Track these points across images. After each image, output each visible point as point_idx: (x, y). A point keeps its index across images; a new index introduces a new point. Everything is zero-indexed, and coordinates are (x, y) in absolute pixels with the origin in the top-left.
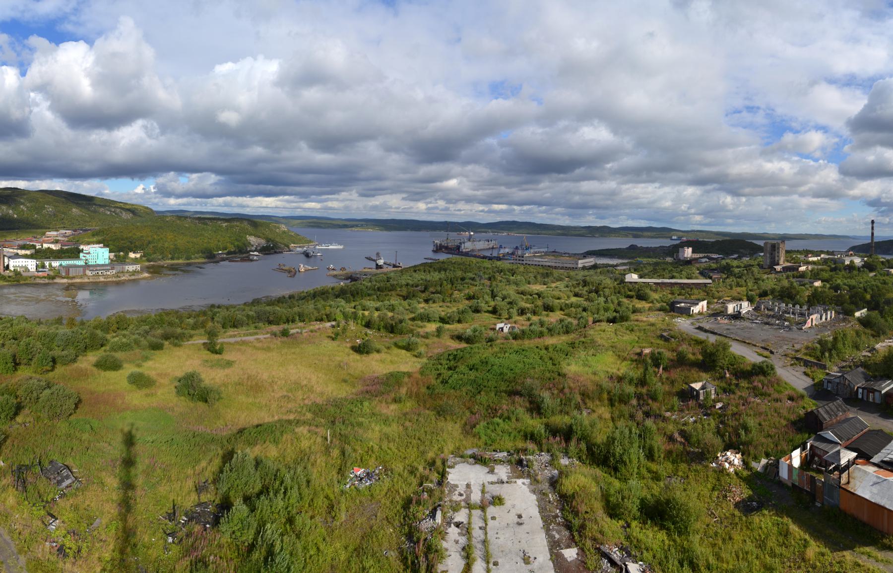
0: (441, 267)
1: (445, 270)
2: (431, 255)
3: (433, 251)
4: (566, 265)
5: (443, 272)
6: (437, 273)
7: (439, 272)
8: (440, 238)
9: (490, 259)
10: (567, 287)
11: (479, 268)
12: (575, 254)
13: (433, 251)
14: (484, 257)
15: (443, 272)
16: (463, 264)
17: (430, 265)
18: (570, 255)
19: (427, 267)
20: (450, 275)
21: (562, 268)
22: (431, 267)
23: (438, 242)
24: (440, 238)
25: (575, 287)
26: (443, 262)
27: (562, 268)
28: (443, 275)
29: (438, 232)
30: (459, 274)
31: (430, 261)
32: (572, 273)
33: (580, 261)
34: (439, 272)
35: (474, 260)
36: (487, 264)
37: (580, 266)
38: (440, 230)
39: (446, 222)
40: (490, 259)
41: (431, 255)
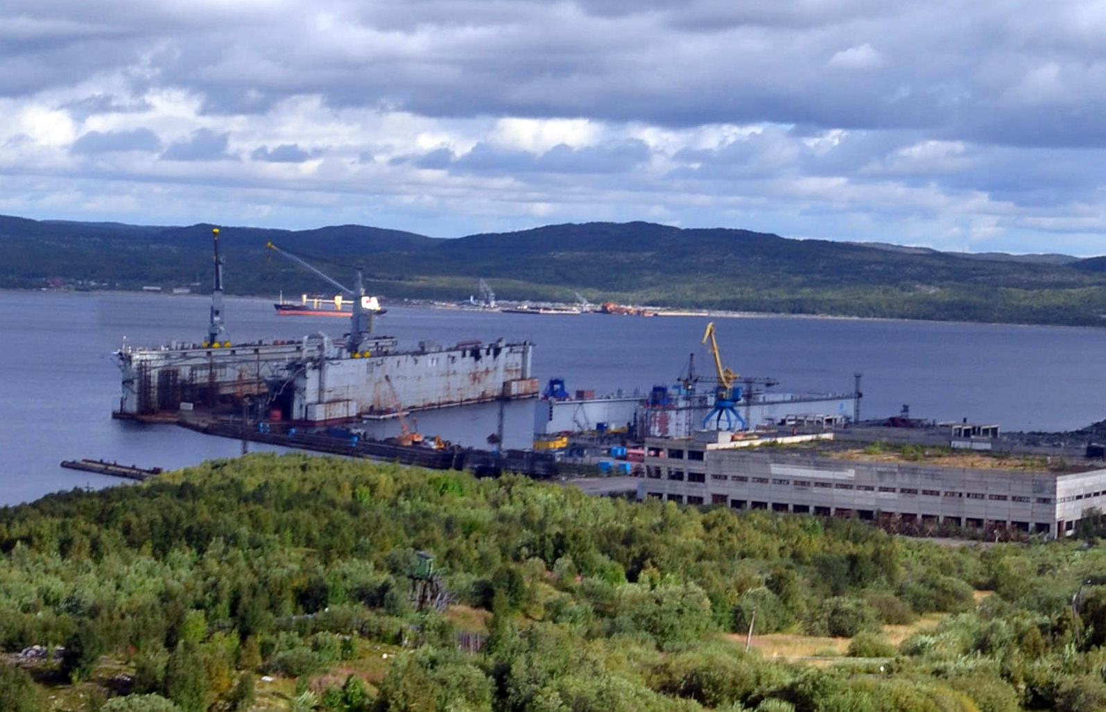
0: (170, 521)
1: (198, 539)
2: (104, 440)
3: (121, 416)
4: (972, 509)
5: (183, 555)
6: (145, 560)
7: (161, 551)
8: (164, 333)
9: (488, 466)
10: (983, 646)
11: (417, 523)
12: (1034, 439)
13: (121, 416)
14: (449, 458)
15: (183, 555)
16: (313, 498)
17: (104, 509)
18: (1002, 445)
19: (87, 518)
20: (229, 569)
21: (951, 527)
22: (105, 519)
23: (150, 358)
24: (164, 333)
25: (1034, 652)
26: (184, 491)
27: (951, 527)
28: (181, 570)
29: (149, 298)
30: (289, 563)
31: (98, 483)
32: (1015, 561)
33: (1066, 485)
34: (161, 551)
35: (383, 474)
36: (468, 499)
37: (1066, 511)
38: (169, 277)
39: (202, 234)
40: (488, 466)
41: (104, 440)
